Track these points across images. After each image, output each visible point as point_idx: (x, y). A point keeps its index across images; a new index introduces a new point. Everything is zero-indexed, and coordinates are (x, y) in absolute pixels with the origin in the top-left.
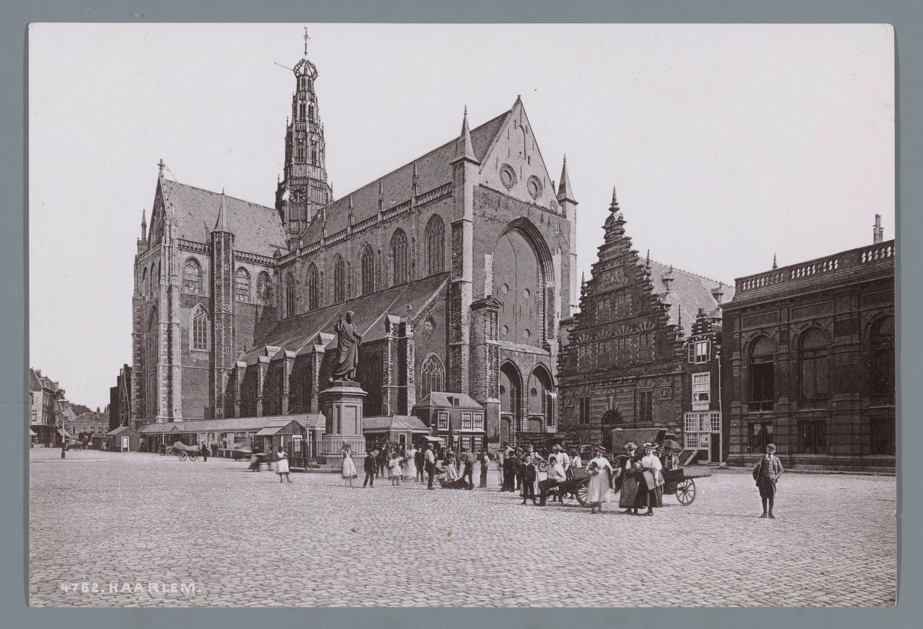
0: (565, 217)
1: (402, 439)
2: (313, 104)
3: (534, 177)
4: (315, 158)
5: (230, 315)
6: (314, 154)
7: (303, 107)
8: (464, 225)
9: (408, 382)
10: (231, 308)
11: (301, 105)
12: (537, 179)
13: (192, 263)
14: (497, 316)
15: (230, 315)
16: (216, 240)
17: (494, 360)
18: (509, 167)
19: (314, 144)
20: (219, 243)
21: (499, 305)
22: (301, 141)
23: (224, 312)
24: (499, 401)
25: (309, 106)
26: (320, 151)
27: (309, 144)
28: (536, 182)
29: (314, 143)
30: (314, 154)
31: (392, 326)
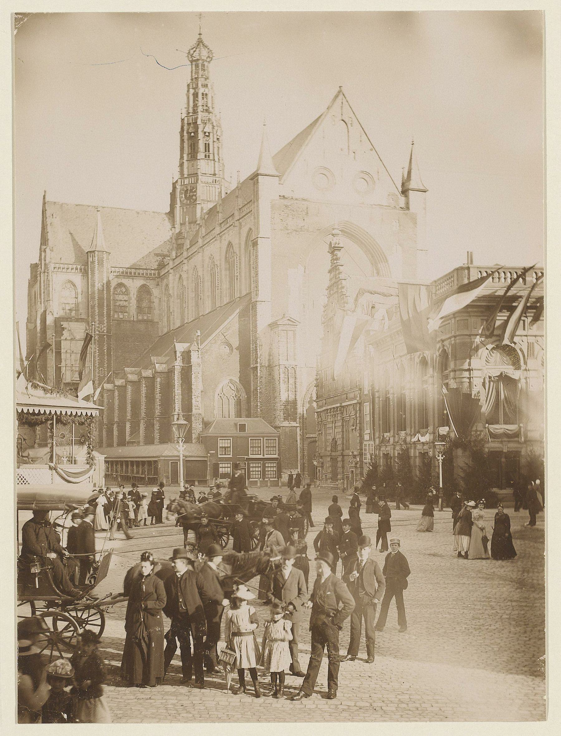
0: (408, 208)
1: (175, 465)
2: (207, 91)
3: (362, 172)
4: (209, 151)
5: (104, 335)
6: (207, 147)
7: (196, 95)
8: (260, 241)
9: (193, 409)
10: (105, 328)
11: (193, 94)
12: (368, 173)
13: (69, 285)
14: (294, 335)
15: (104, 335)
16: (90, 259)
17: (291, 381)
18: (325, 168)
19: (207, 135)
20: (93, 262)
21: (297, 323)
22: (192, 134)
23: (97, 332)
24: (298, 425)
25: (203, 94)
26: (214, 141)
27: (201, 135)
28: (366, 177)
29: (207, 134)
30: (207, 147)
31: (178, 354)
